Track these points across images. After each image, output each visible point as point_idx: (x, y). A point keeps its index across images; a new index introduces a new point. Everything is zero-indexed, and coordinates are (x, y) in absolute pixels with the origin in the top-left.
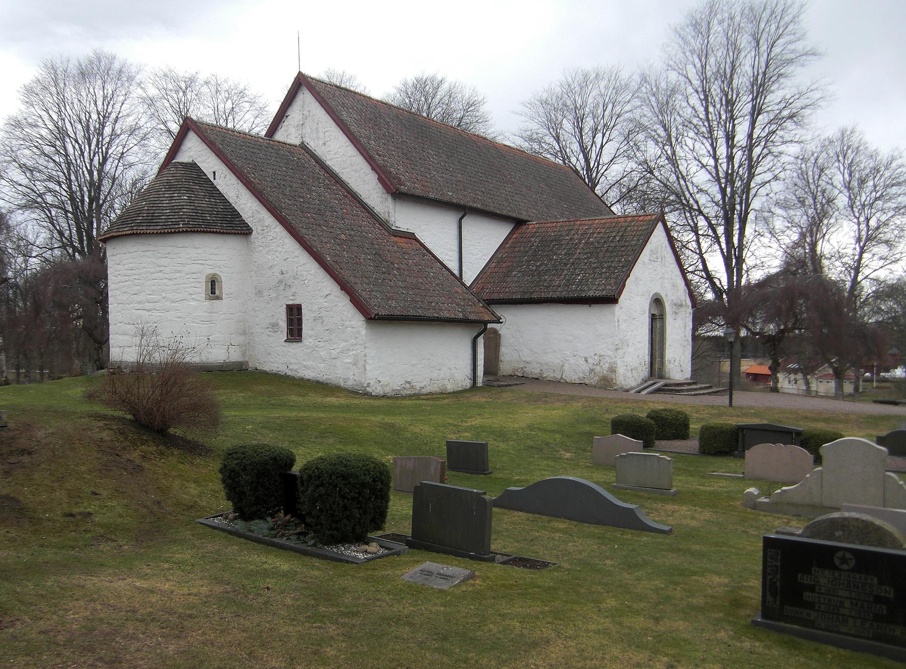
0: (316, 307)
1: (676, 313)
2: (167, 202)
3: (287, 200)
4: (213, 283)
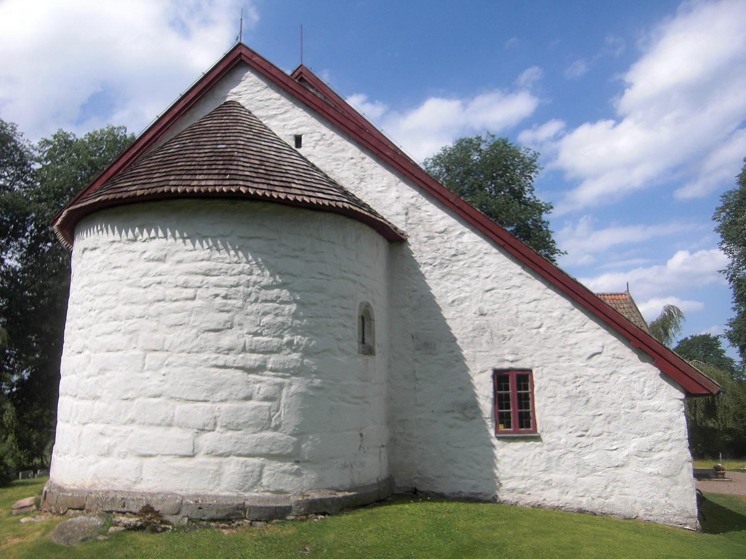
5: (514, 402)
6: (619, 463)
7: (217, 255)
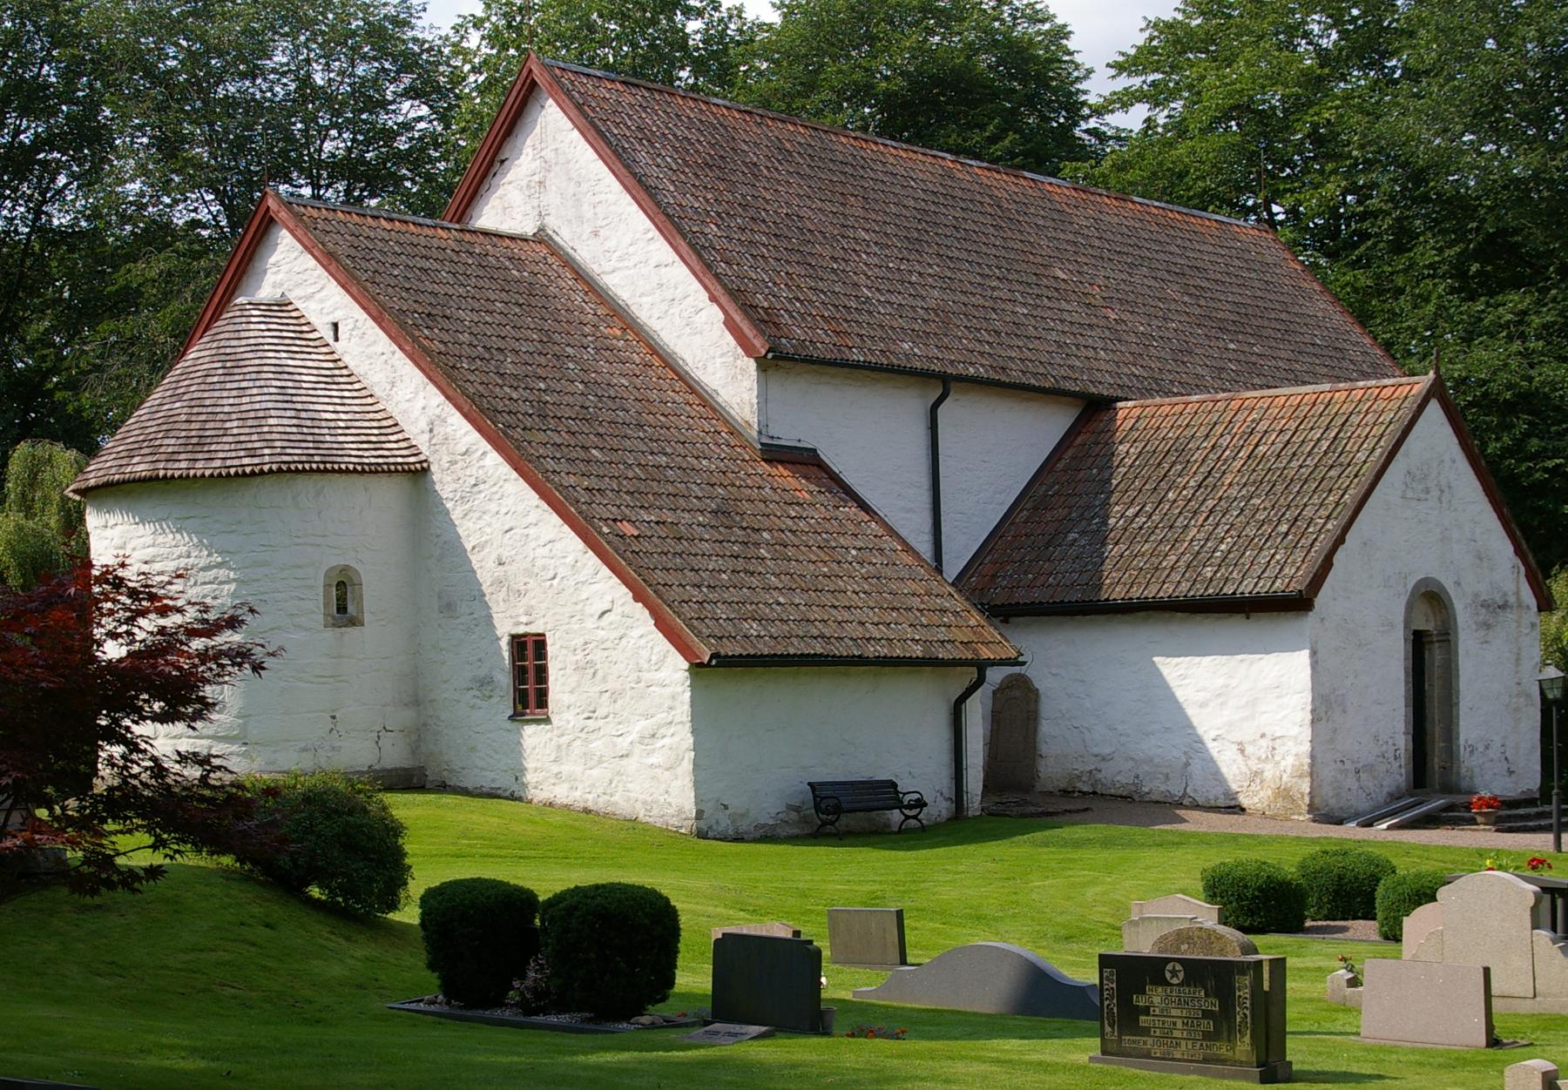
0: (579, 641)
1: (1487, 626)
2: (231, 401)
3: (507, 389)
4: (341, 585)
5: (531, 675)
6: (625, 752)
7: (161, 539)
